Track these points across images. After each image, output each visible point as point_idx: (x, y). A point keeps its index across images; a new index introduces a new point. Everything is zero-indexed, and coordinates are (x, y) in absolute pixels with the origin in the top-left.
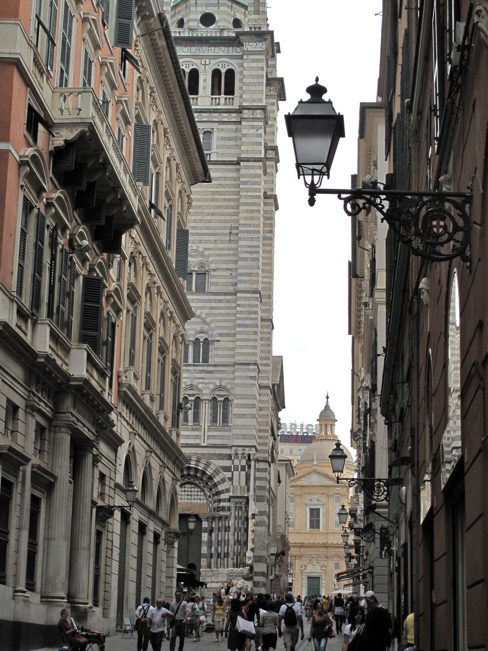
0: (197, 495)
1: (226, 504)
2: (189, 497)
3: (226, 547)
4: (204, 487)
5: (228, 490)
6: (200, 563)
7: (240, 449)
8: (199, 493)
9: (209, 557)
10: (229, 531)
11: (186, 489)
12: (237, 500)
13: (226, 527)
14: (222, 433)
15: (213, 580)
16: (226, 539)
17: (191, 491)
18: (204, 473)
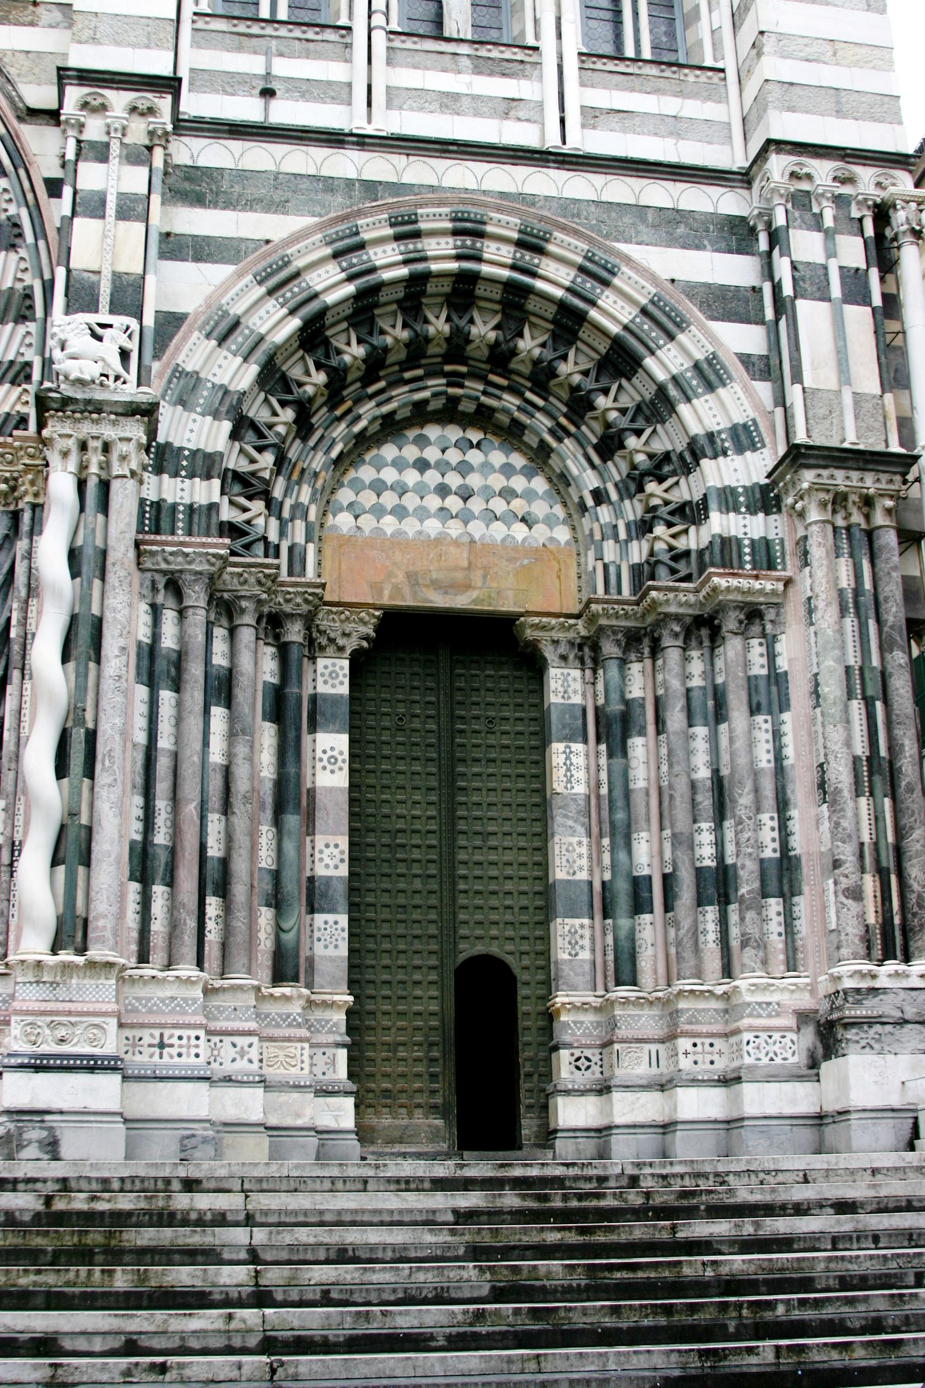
0: (508, 494)
1: (751, 527)
2: (454, 503)
3: (768, 819)
4: (559, 432)
5: (744, 438)
6: (545, 954)
7: (823, 171)
8: (519, 483)
9: (623, 901)
10: (784, 705)
11: (432, 454)
12: (840, 478)
13: (751, 683)
14: (670, 105)
15: (685, 1063)
16: (764, 759)
17: (464, 469)
18: (569, 322)
